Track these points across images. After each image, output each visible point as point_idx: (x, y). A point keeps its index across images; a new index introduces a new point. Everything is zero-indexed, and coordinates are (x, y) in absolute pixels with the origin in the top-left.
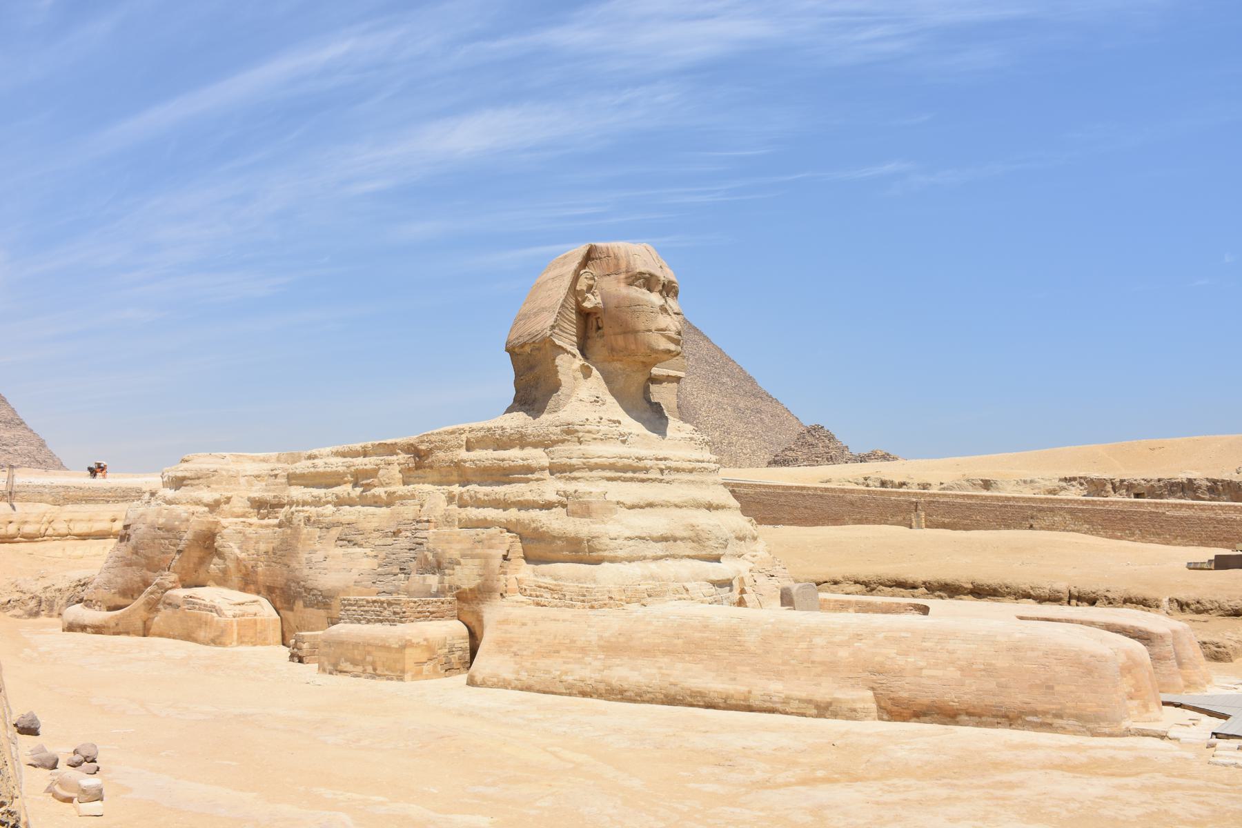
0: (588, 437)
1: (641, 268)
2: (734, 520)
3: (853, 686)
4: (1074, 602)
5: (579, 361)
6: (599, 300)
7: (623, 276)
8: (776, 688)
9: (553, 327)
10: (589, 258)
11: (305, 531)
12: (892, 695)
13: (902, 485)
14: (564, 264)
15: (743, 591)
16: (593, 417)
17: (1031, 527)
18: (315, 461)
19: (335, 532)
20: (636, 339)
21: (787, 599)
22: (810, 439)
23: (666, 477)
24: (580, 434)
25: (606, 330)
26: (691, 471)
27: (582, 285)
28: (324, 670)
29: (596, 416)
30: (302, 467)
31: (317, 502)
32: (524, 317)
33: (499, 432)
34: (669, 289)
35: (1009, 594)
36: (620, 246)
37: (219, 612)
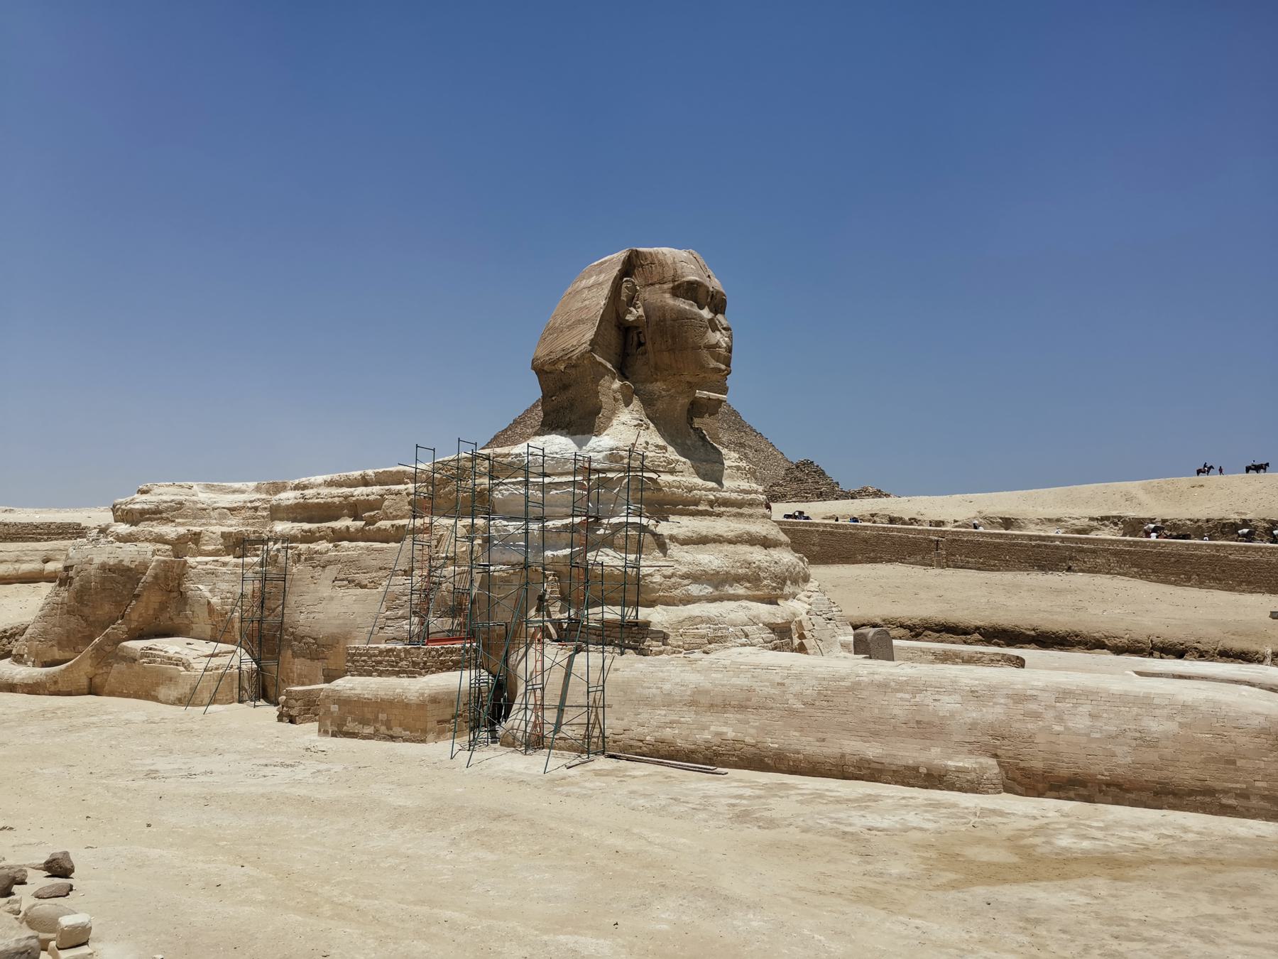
2: (787, 558)
3: (971, 752)
4: (1156, 654)
8: (873, 751)
10: (631, 265)
11: (295, 570)
12: (1022, 765)
13: (913, 521)
14: (600, 272)
15: (802, 636)
17: (1069, 569)
18: (306, 492)
19: (332, 571)
21: (861, 646)
22: (800, 475)
23: (717, 509)
26: (740, 504)
28: (326, 732)
30: (288, 497)
31: (309, 537)
35: (1079, 643)
36: (667, 253)
37: (187, 666)
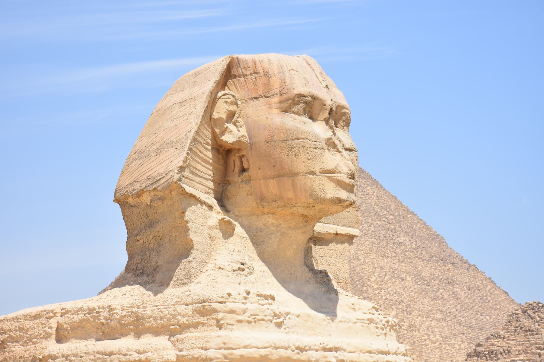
0: (230, 318)
1: (299, 87)
5: (217, 215)
6: (243, 131)
7: (275, 99)
9: (182, 169)
10: (228, 75)
14: (195, 84)
16: (238, 291)
20: (294, 185)
24: (220, 315)
25: (253, 172)
27: (221, 111)
29: (242, 289)
32: (140, 155)
33: (106, 314)
34: (337, 117)
36: (272, 60)
